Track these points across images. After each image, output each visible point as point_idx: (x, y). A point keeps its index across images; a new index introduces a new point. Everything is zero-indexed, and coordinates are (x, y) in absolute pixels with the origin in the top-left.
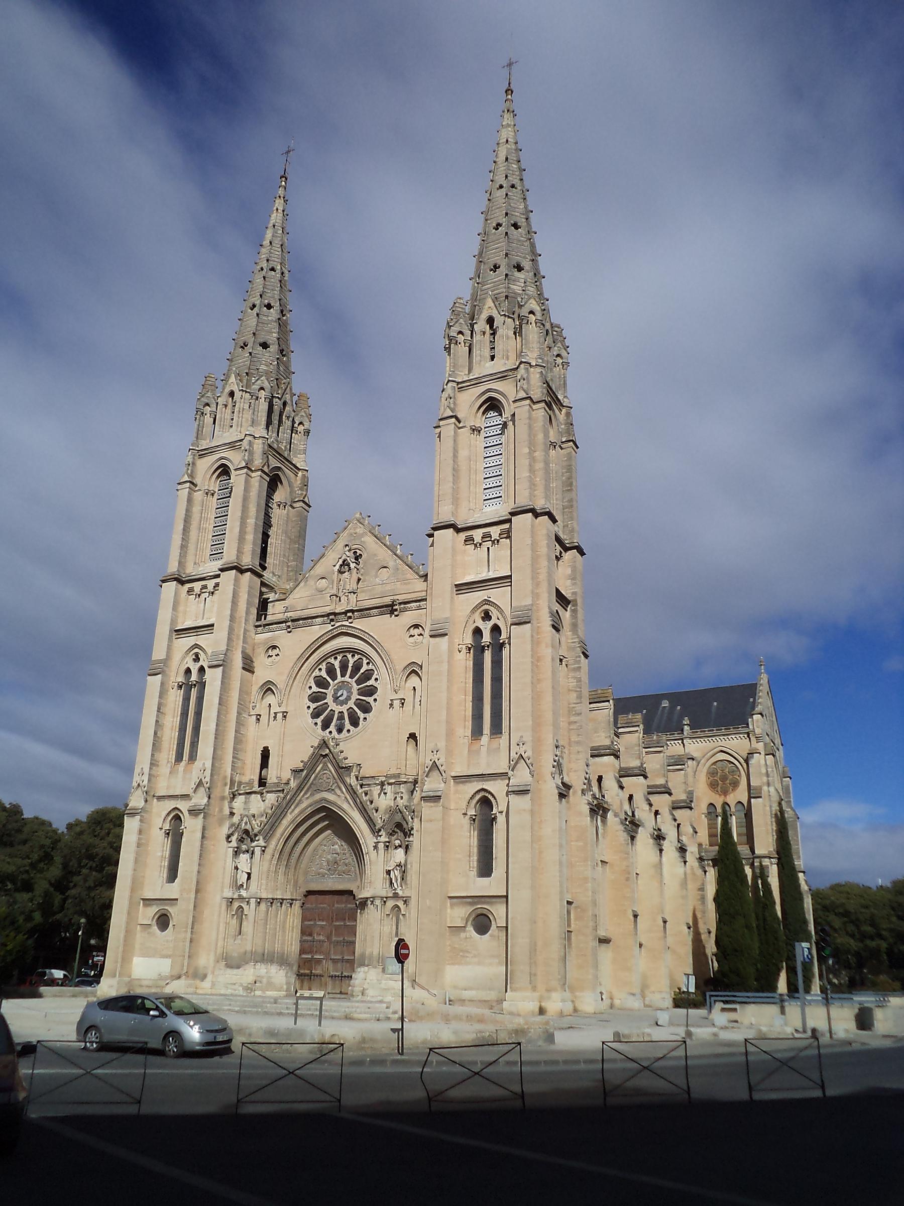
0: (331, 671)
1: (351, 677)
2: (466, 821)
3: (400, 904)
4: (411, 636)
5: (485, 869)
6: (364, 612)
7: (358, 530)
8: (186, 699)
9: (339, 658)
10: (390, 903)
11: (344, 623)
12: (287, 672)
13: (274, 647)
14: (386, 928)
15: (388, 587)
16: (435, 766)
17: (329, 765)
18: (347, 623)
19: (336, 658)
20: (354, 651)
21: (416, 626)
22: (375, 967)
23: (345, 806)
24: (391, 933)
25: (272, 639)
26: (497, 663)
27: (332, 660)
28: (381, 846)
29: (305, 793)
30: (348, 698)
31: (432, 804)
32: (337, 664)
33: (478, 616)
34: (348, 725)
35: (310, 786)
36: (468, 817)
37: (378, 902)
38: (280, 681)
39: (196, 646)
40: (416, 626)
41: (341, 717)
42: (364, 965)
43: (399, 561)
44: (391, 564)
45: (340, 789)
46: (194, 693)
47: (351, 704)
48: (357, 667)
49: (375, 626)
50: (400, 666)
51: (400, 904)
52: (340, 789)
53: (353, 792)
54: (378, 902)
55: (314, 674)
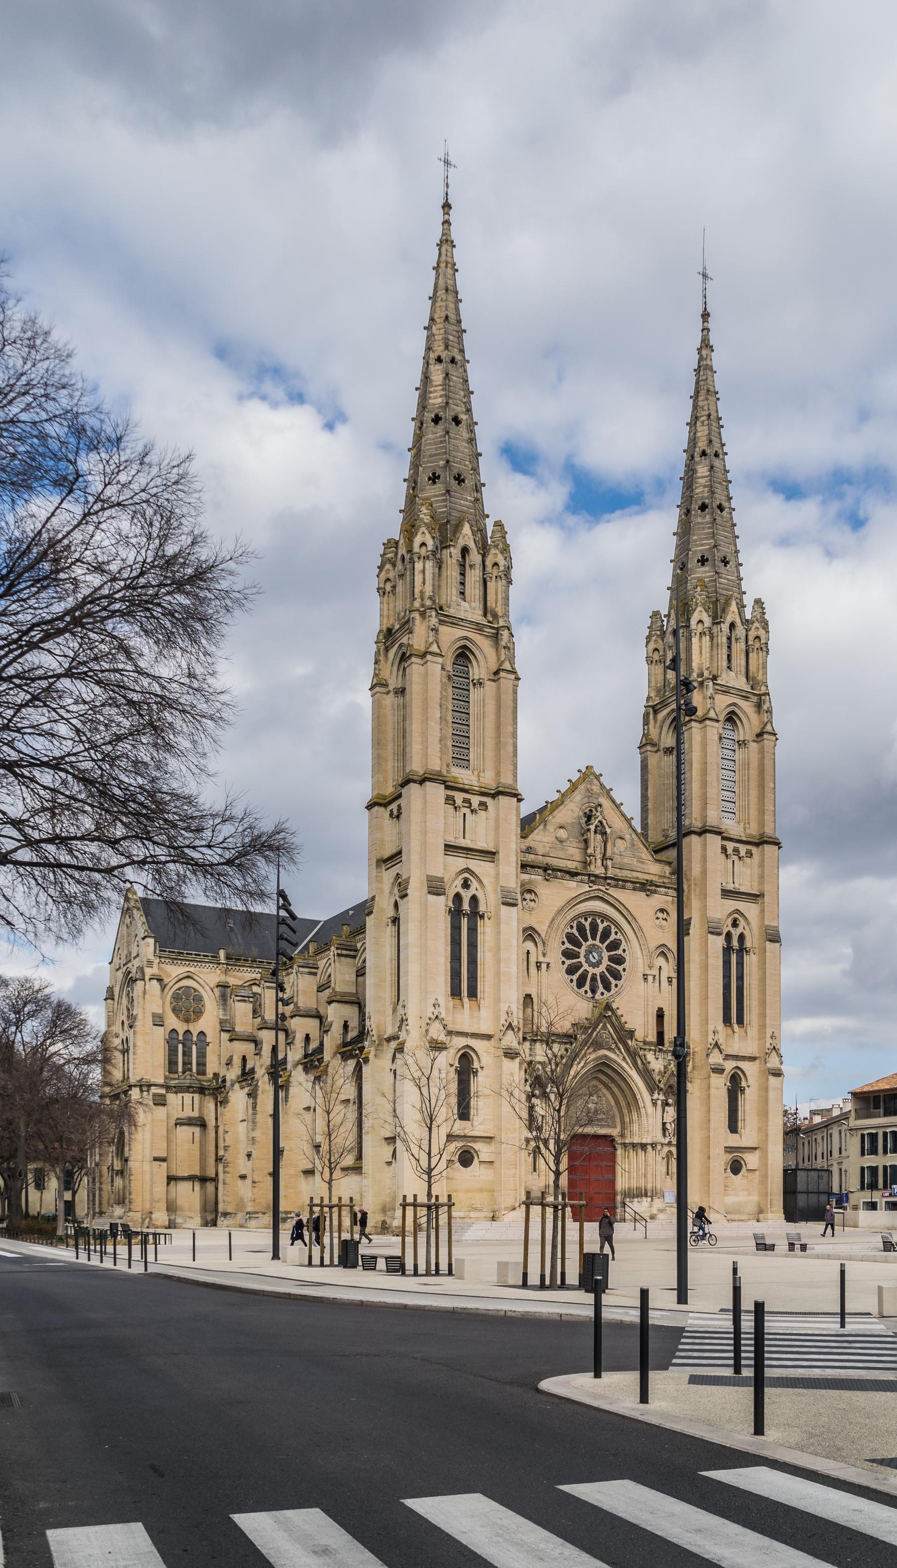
0: (581, 929)
1: (602, 941)
4: (658, 918)
5: (733, 1127)
6: (620, 883)
7: (594, 788)
8: (456, 928)
9: (589, 920)
11: (600, 887)
12: (548, 922)
13: (530, 891)
15: (625, 861)
16: (717, 1045)
18: (603, 888)
19: (586, 919)
20: (605, 917)
21: (662, 910)
23: (624, 1064)
25: (530, 882)
26: (740, 964)
27: (583, 921)
28: (659, 1103)
29: (588, 1048)
30: (599, 963)
32: (587, 925)
33: (730, 921)
34: (601, 989)
35: (592, 1043)
37: (659, 1147)
38: (542, 929)
39: (467, 870)
40: (662, 910)
41: (594, 978)
42: (646, 1196)
43: (634, 836)
44: (627, 837)
45: (619, 1049)
46: (464, 923)
47: (585, 966)
48: (606, 934)
49: (630, 899)
50: (653, 945)
53: (633, 1055)
55: (566, 931)
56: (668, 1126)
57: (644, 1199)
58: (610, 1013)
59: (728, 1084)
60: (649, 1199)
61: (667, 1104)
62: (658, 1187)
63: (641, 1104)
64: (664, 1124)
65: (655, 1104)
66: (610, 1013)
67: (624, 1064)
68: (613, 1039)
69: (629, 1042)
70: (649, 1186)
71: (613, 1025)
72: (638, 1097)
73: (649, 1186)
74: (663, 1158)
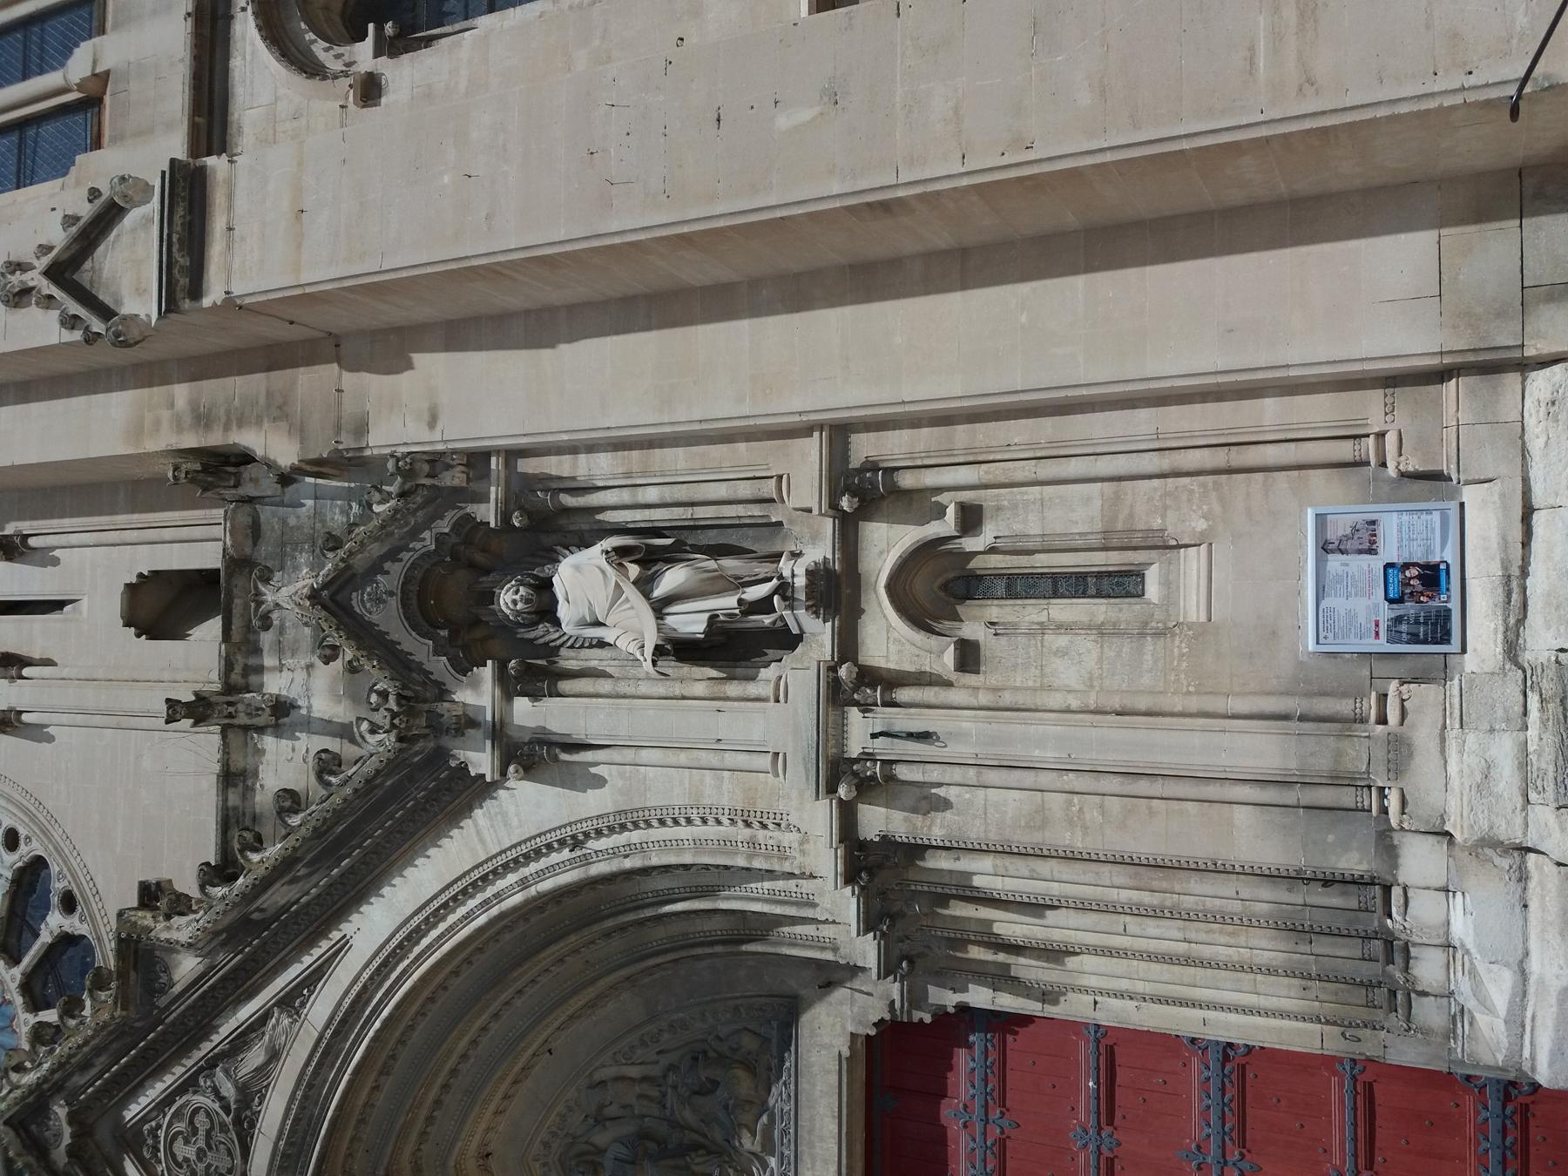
2: (404, 76)
3: (887, 544)
10: (887, 639)
14: (1067, 674)
17: (132, 1112)
22: (1399, 753)
23: (321, 1008)
24: (1102, 631)
31: (218, 224)
36: (386, 67)
37: (859, 731)
42: (1379, 888)
45: (241, 1041)
51: (887, 544)
52: (241, 1041)
54: (859, 731)
56: (690, 621)
57: (1420, 914)
58: (60, 1111)
59: (363, 54)
60: (1419, 862)
61: (544, 607)
62: (1262, 750)
63: (558, 873)
64: (678, 650)
65: (536, 756)
66: (60, 1111)
67: (321, 1008)
68: (189, 1085)
69: (187, 966)
70: (1253, 838)
71: (128, 1083)
72: (510, 893)
73: (1253, 838)
74: (969, 658)
